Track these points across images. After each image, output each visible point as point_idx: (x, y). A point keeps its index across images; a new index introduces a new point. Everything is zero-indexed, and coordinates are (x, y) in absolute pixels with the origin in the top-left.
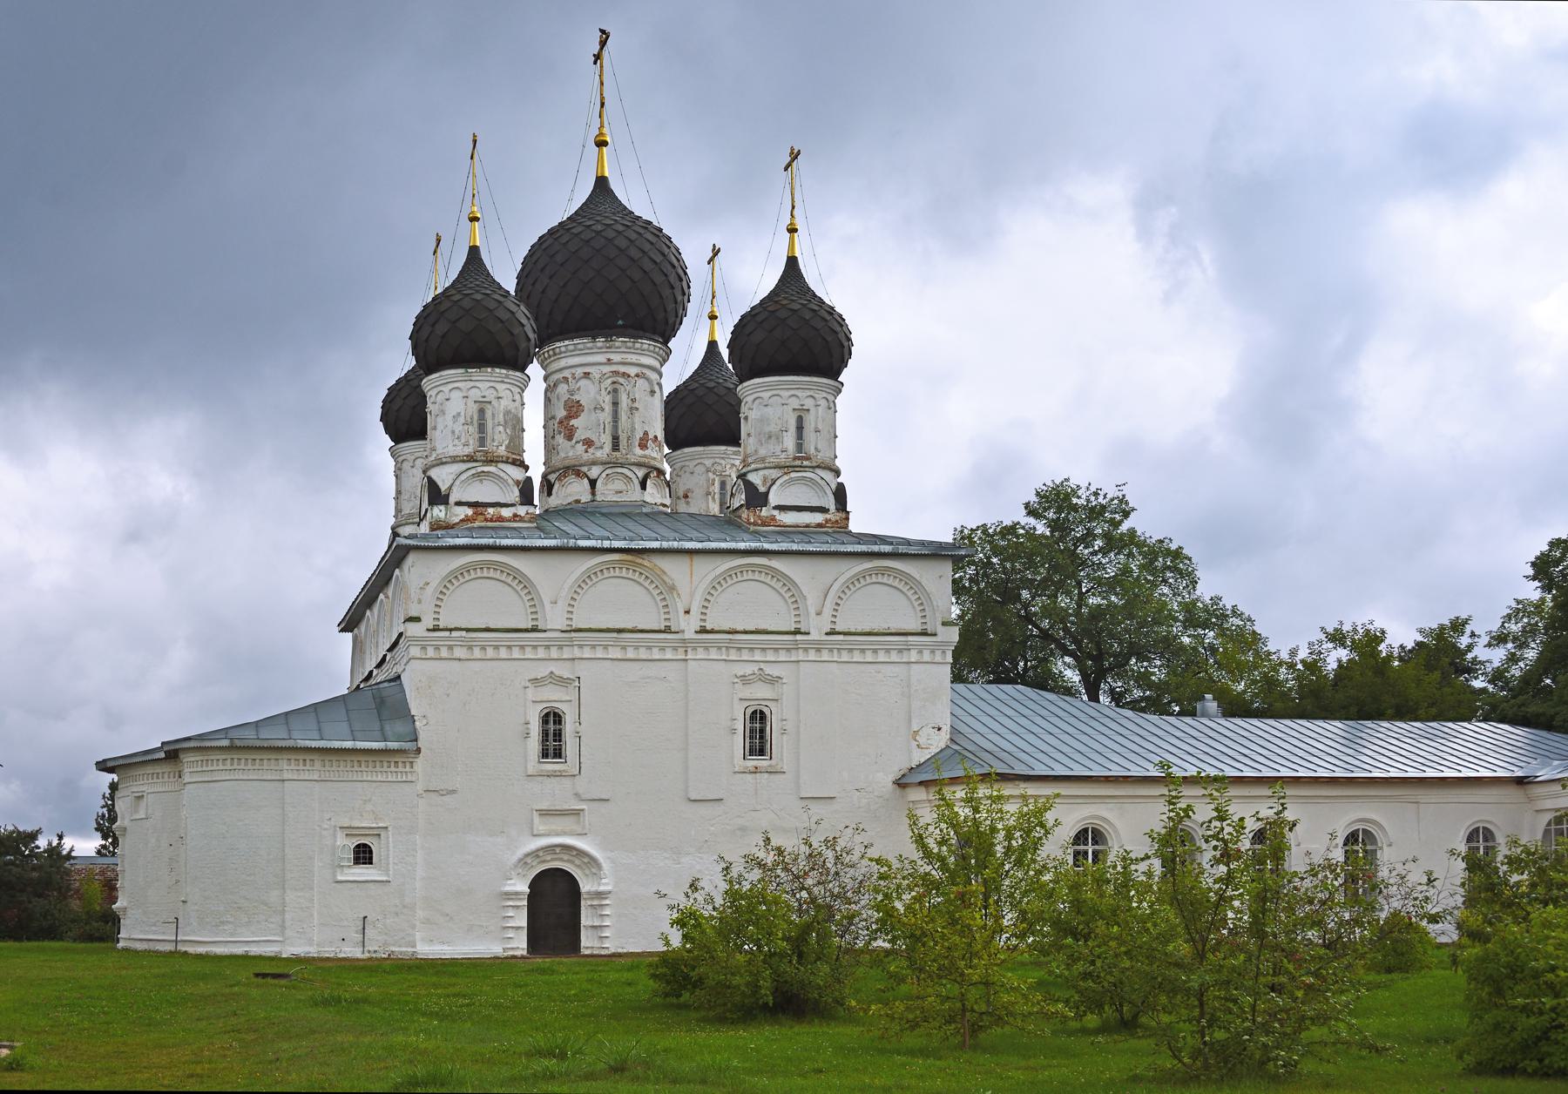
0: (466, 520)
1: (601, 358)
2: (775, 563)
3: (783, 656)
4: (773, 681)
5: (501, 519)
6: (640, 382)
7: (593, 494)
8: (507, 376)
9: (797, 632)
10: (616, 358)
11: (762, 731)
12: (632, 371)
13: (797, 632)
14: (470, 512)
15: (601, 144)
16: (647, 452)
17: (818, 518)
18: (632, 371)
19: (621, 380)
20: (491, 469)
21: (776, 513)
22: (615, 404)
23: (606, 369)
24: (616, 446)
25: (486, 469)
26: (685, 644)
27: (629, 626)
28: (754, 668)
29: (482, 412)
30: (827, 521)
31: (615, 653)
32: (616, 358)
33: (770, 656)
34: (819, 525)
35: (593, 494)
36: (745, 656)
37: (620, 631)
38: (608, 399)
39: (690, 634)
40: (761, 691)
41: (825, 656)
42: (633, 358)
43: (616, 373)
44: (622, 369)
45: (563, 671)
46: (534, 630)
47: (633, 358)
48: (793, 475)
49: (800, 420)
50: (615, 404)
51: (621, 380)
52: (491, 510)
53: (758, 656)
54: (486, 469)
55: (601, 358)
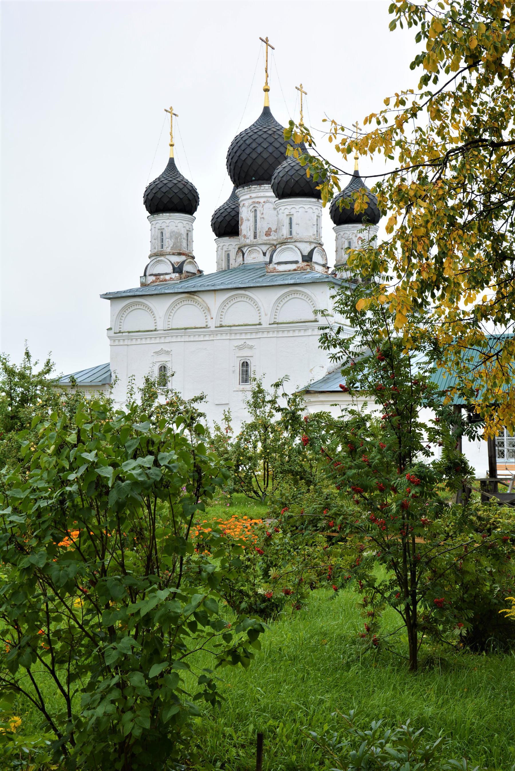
0: (153, 282)
1: (248, 196)
2: (247, 293)
3: (254, 336)
4: (251, 347)
5: (166, 280)
6: (267, 205)
7: (243, 260)
8: (170, 216)
9: (260, 324)
10: (253, 195)
11: (247, 371)
12: (262, 200)
13: (260, 324)
14: (154, 278)
15: (266, 90)
16: (270, 237)
17: (294, 266)
18: (262, 200)
19: (257, 205)
20: (162, 258)
21: (276, 266)
22: (255, 217)
23: (251, 201)
24: (255, 237)
25: (160, 259)
26: (212, 333)
27: (193, 326)
28: (242, 342)
29: (162, 233)
30: (298, 267)
31: (187, 339)
32: (253, 195)
33: (248, 336)
34: (295, 270)
35: (243, 260)
36: (238, 336)
37: (186, 329)
38: (252, 215)
39: (213, 328)
40: (246, 353)
41: (271, 335)
42: (262, 194)
43: (254, 202)
44: (257, 200)
45: (166, 348)
46: (155, 330)
47: (262, 194)
48: (283, 247)
49: (291, 219)
50: (255, 217)
51: (257, 205)
52: (162, 277)
53: (243, 336)
54: (160, 259)
55: (248, 196)
